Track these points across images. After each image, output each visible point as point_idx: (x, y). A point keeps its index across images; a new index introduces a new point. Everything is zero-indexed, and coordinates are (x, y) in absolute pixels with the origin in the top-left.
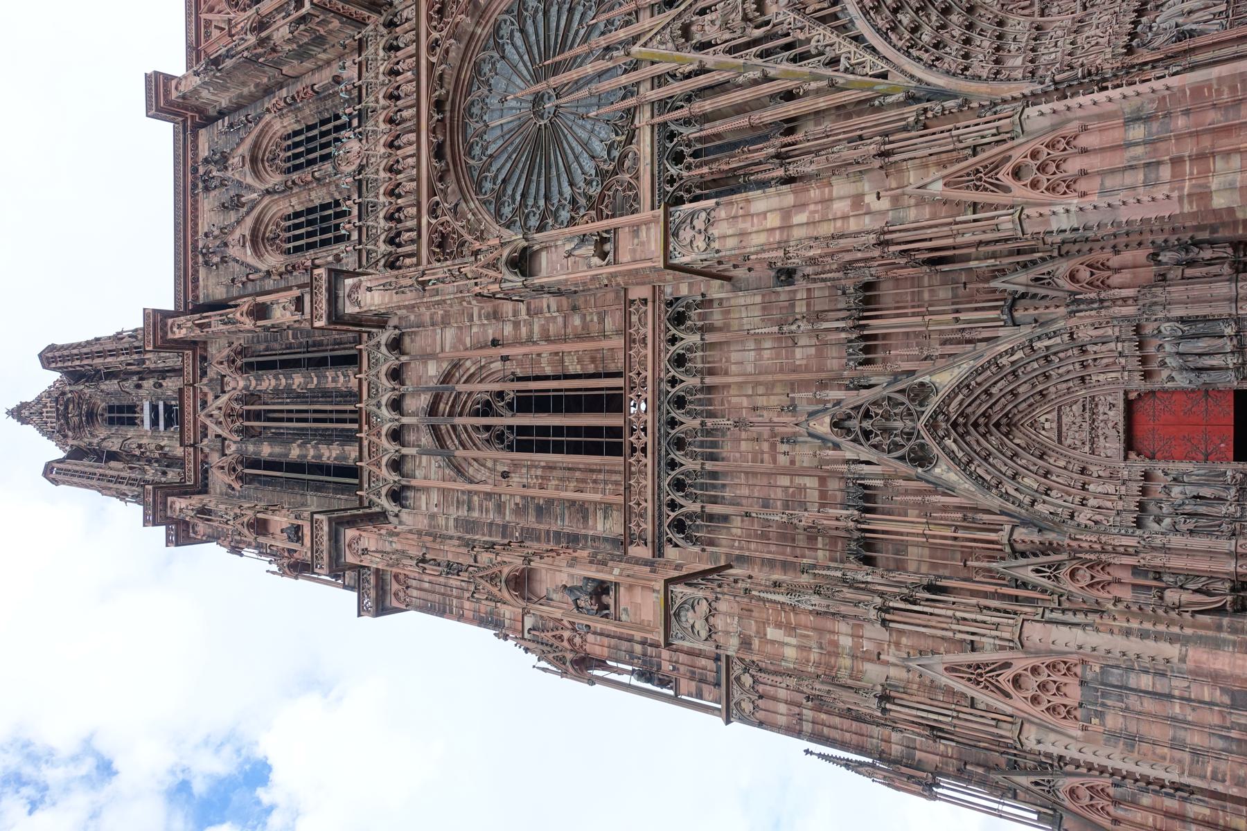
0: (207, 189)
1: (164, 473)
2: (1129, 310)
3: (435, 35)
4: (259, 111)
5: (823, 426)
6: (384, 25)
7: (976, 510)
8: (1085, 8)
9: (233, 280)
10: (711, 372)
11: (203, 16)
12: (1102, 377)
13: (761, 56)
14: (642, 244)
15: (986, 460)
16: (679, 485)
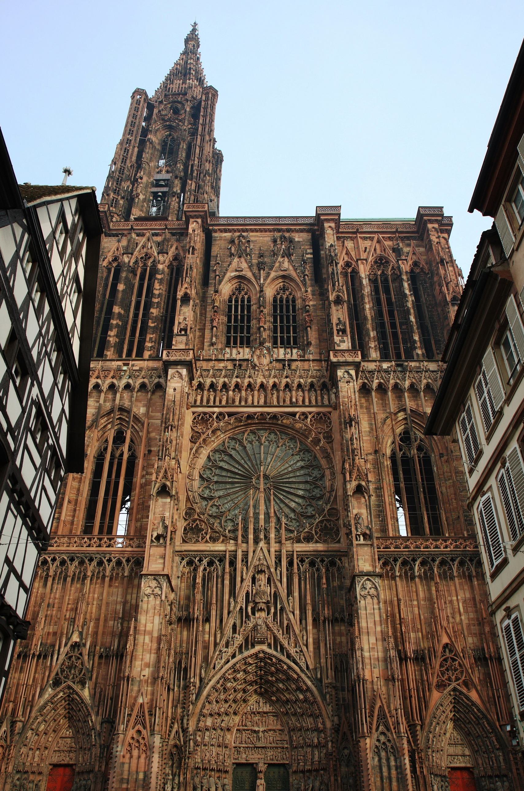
0: (275, 241)
1: (123, 198)
2: (97, 768)
3: (310, 417)
4: (308, 282)
5: (76, 638)
6: (324, 382)
7: (32, 707)
8: (234, 747)
9: (218, 263)
10: (111, 579)
11: (376, 236)
12: (81, 756)
13: (241, 609)
14: (156, 560)
15: (53, 709)
16: (63, 562)
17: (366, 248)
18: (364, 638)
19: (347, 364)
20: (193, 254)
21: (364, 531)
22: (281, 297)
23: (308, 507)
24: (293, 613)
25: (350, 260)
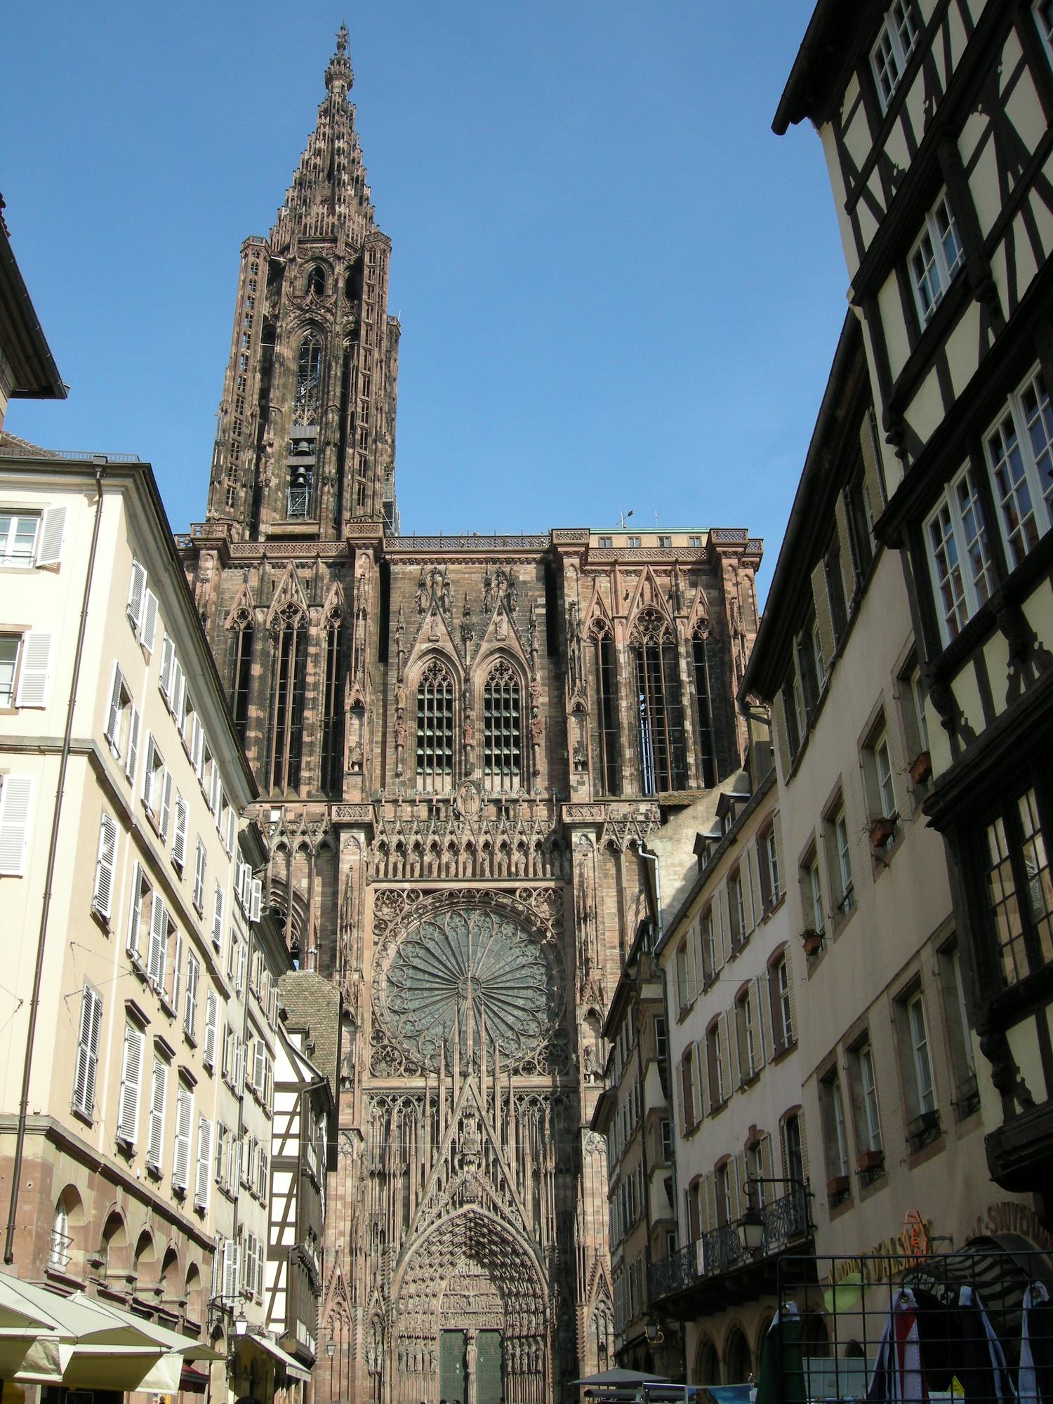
0: (488, 584)
1: (244, 486)
3: (535, 894)
4: (537, 660)
9: (402, 628)
11: (645, 569)
13: (446, 1161)
17: (627, 595)
18: (588, 1200)
19: (585, 825)
20: (365, 619)
21: (595, 1069)
22: (497, 684)
23: (530, 1023)
24: (509, 1165)
25: (602, 617)
